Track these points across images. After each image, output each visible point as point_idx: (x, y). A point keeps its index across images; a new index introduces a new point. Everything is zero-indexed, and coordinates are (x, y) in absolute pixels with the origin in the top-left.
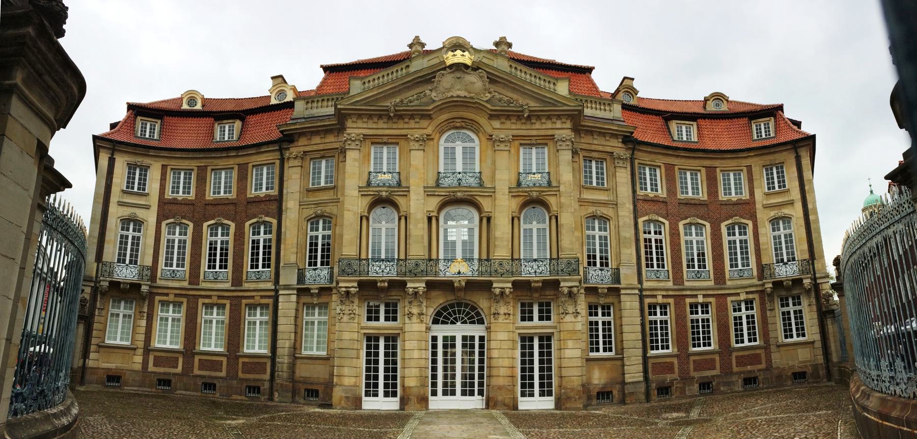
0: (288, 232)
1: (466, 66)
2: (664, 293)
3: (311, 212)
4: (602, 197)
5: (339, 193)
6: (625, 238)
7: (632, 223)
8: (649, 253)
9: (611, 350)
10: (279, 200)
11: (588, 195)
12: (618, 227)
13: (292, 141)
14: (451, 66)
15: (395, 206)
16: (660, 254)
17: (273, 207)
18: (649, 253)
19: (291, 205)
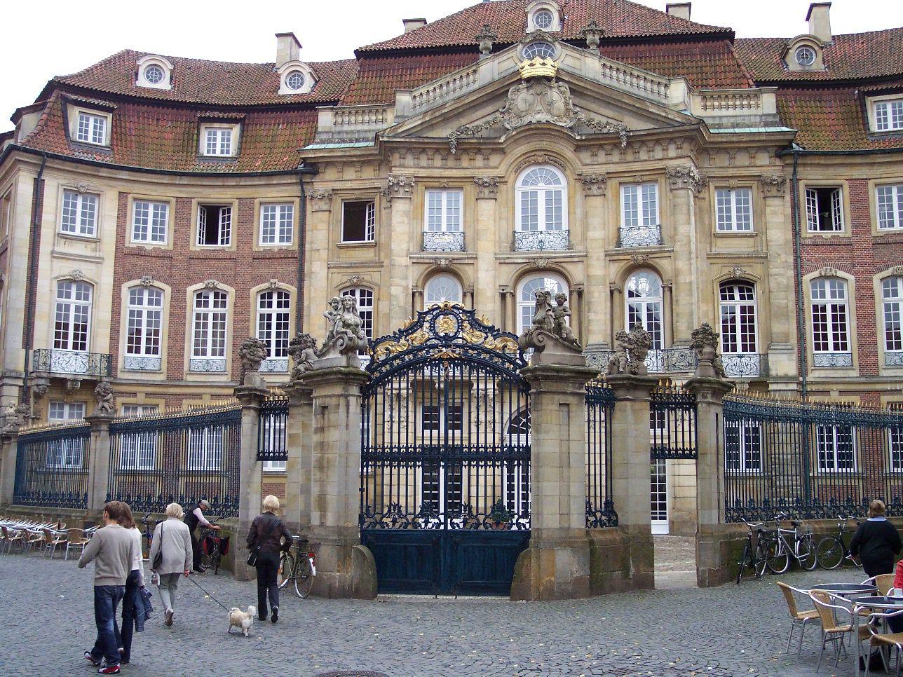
0: (313, 307)
1: (548, 79)
2: (841, 387)
3: (345, 279)
4: (743, 246)
5: (382, 254)
6: (779, 307)
7: (792, 283)
8: (820, 327)
9: (757, 465)
10: (299, 258)
11: (722, 247)
12: (768, 293)
13: (315, 173)
14: (528, 80)
15: (456, 274)
16: (840, 326)
17: (292, 267)
18: (820, 327)
19: (318, 270)
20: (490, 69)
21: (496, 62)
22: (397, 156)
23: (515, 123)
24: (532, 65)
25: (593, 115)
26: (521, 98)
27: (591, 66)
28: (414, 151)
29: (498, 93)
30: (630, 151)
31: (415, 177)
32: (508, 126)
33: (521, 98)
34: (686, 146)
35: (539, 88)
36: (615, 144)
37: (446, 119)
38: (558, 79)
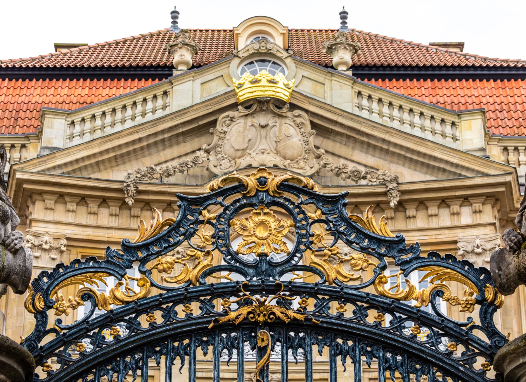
20: (187, 94)
21: (199, 81)
22: (39, 205)
23: (226, 165)
24: (255, 81)
25: (342, 162)
26: (237, 132)
27: (340, 95)
28: (67, 199)
29: (202, 125)
30: (400, 215)
31: (68, 239)
32: (216, 171)
33: (237, 132)
34: (488, 209)
35: (262, 119)
36: (378, 204)
37: (121, 156)
38: (293, 107)
